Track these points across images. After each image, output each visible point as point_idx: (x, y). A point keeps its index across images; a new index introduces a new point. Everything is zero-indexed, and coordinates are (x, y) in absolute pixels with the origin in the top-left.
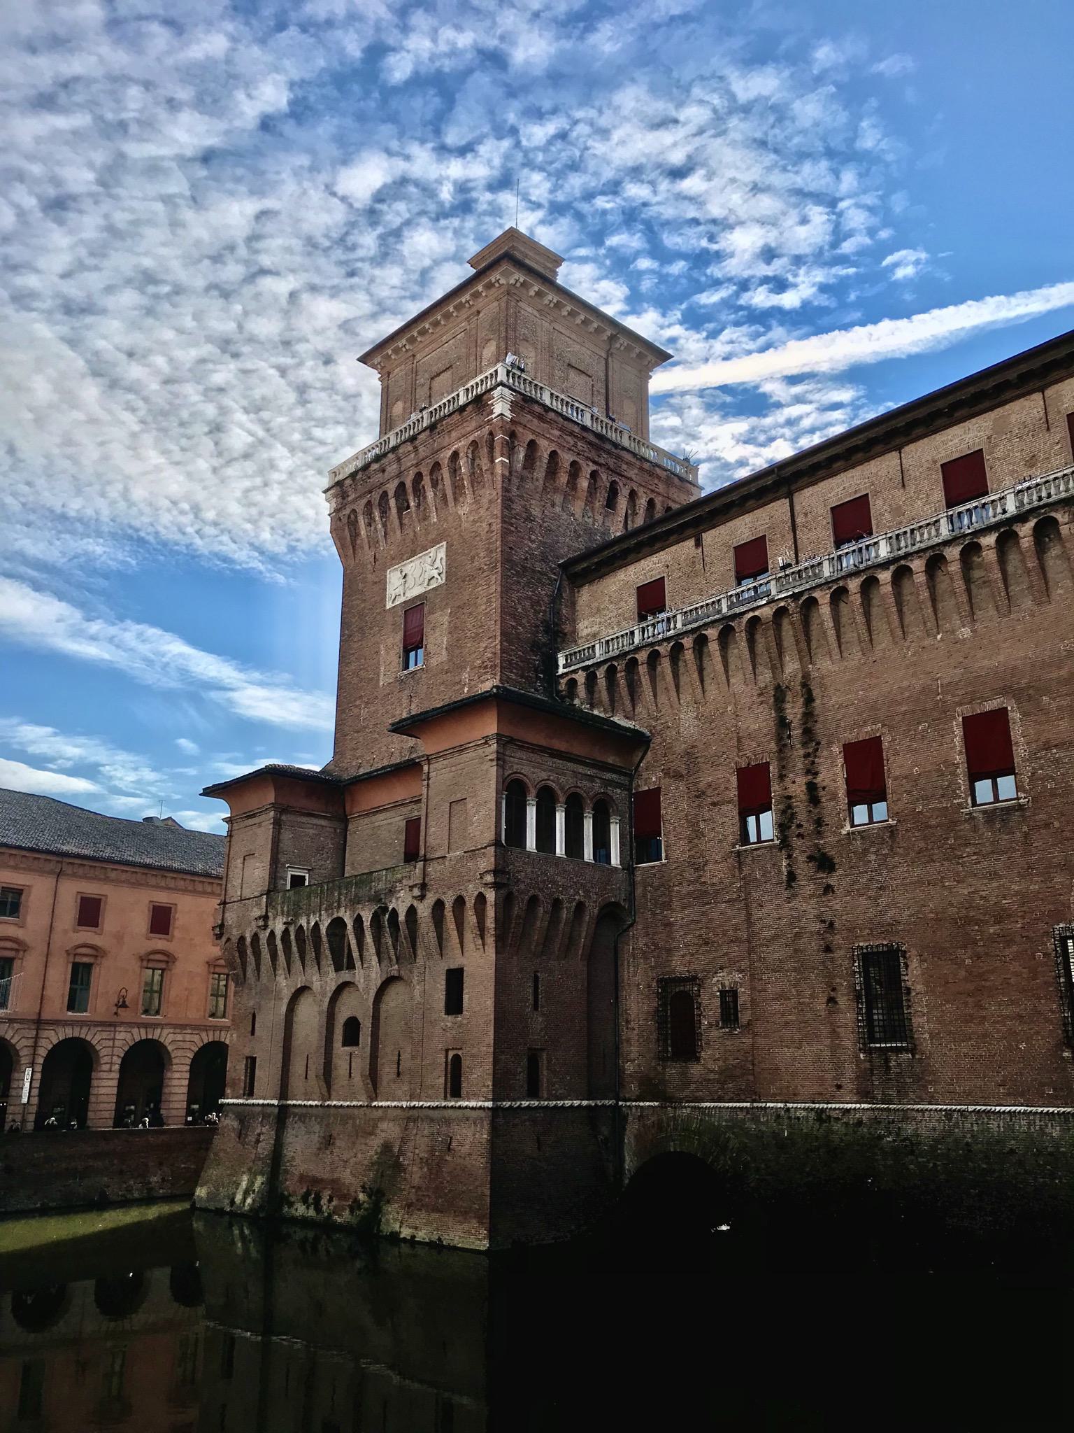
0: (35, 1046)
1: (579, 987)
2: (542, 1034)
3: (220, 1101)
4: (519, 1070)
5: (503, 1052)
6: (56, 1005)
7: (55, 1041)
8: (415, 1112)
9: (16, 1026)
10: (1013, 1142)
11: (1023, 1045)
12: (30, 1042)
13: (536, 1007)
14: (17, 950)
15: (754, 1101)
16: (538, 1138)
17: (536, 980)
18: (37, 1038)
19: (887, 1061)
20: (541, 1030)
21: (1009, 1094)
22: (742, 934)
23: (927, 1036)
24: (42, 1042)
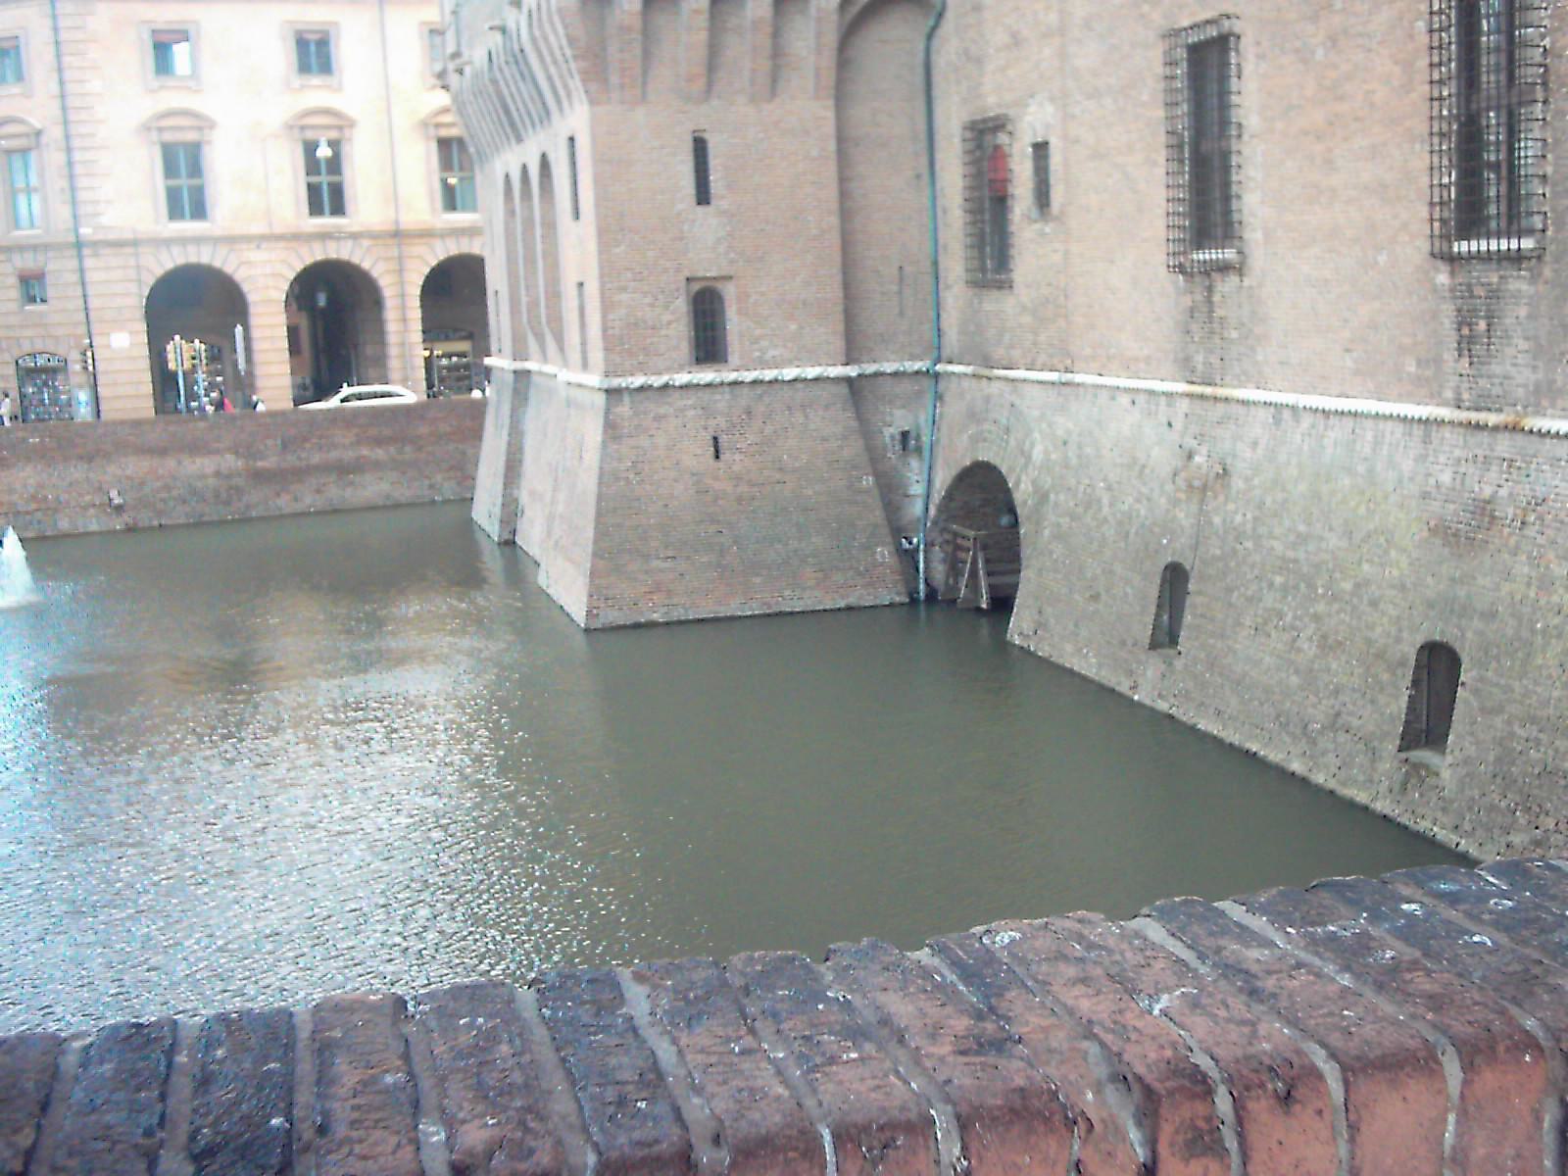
0: (401, 271)
1: (815, 153)
2: (721, 249)
3: (487, 361)
4: (666, 317)
5: (624, 289)
6: (420, 205)
7: (434, 263)
8: (575, 393)
9: (366, 243)
10: (1347, 481)
11: (1382, 259)
12: (393, 266)
13: (703, 196)
14: (340, 128)
15: (1067, 370)
16: (715, 439)
17: (700, 148)
18: (400, 259)
19: (1210, 289)
20: (719, 240)
21: (1357, 372)
22: (1053, 18)
23: (1259, 235)
24: (410, 264)
